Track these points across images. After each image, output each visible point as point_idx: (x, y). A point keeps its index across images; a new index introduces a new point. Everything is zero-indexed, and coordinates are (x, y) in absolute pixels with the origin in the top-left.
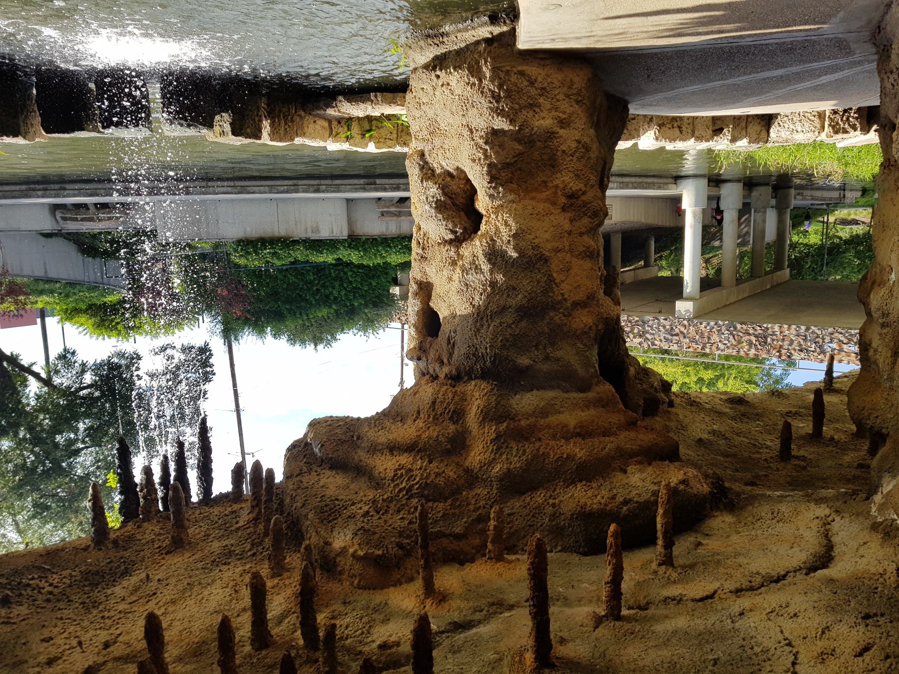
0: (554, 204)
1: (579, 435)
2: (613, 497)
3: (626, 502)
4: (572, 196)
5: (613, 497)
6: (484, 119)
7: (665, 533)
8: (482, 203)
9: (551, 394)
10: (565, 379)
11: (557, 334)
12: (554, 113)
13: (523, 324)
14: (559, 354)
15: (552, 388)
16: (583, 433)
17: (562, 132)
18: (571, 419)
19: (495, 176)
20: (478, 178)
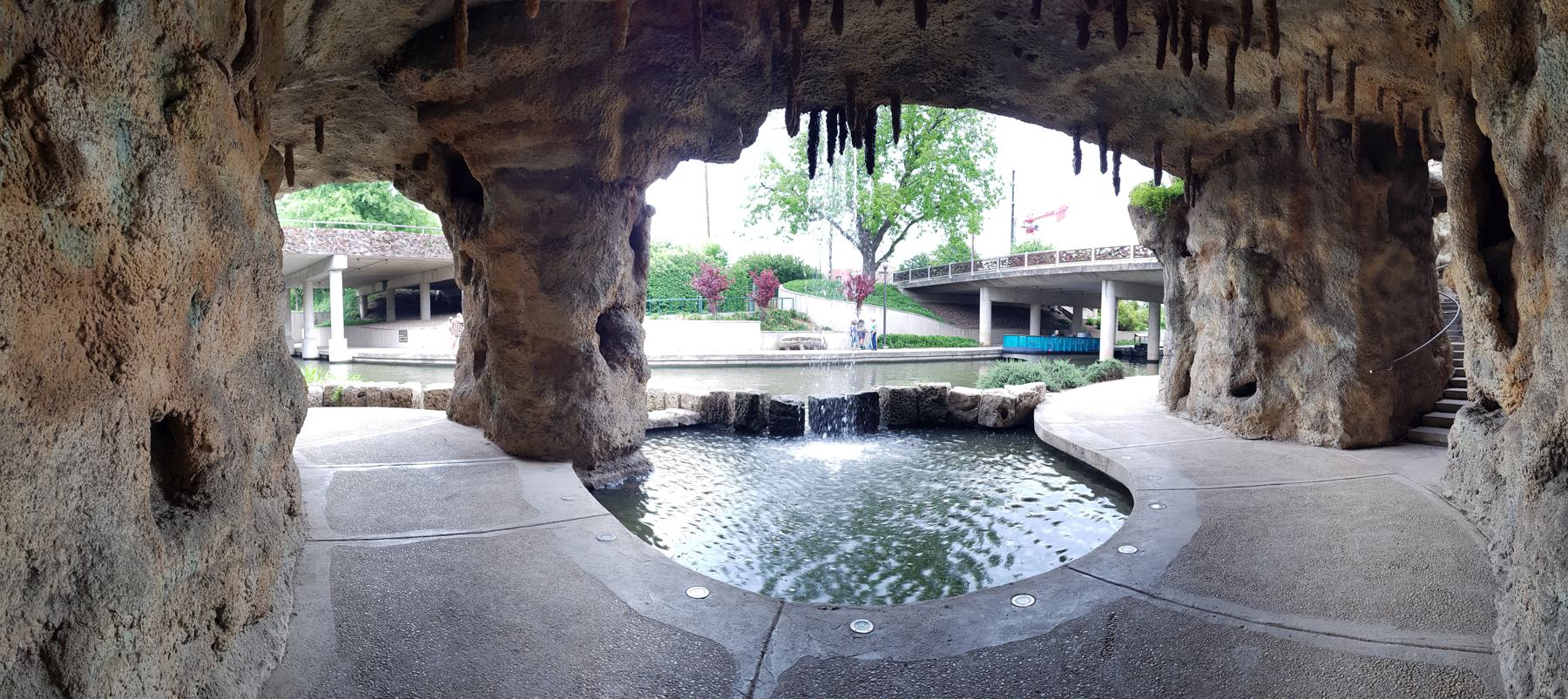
0: (535, 338)
1: (515, 125)
2: (493, 59)
3: (484, 54)
4: (519, 343)
5: (493, 59)
6: (599, 409)
7: (461, 17)
8: (595, 340)
9: (538, 166)
10: (522, 181)
11: (532, 222)
12: (538, 412)
13: (564, 233)
14: (527, 205)
15: (536, 173)
16: (510, 128)
17: (530, 397)
18: (522, 142)
19: (589, 358)
20: (600, 358)
